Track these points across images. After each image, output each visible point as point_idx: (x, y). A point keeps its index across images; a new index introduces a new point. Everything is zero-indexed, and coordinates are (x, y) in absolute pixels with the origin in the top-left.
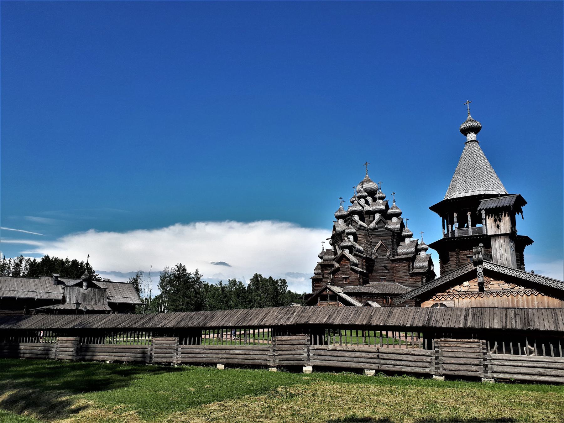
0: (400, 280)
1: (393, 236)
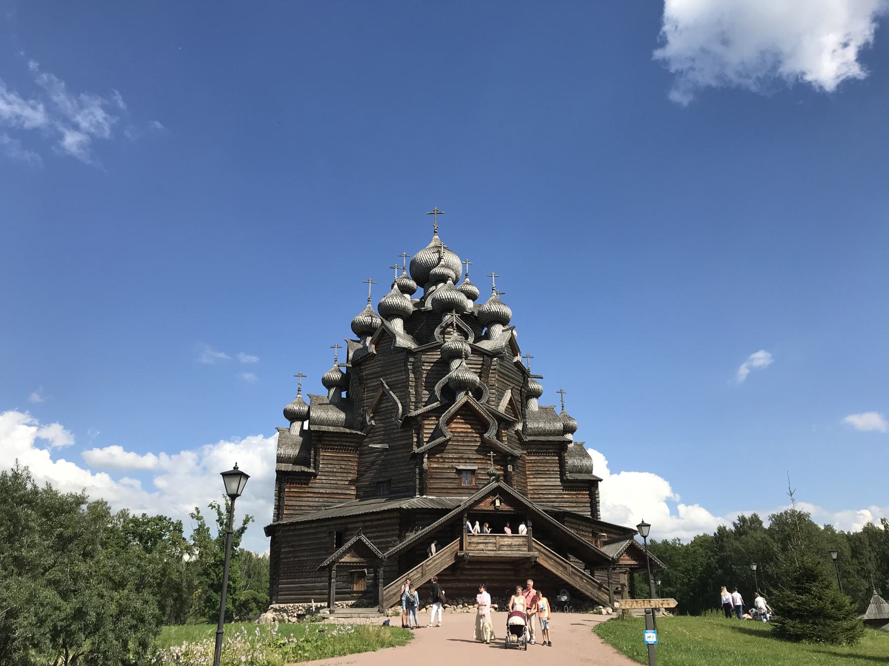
0: (541, 496)
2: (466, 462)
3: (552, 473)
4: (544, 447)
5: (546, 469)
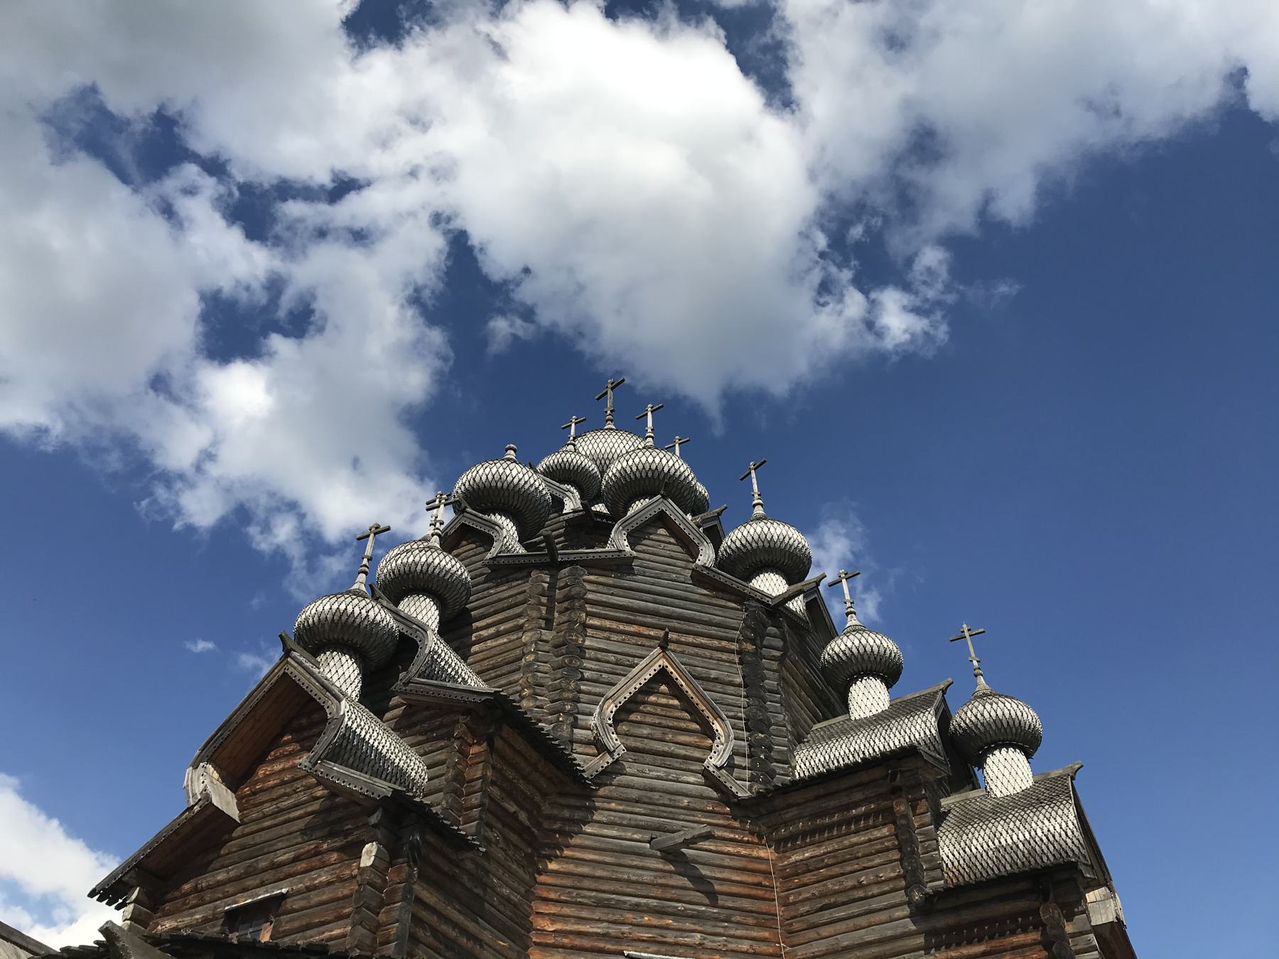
1: (755, 631)
3: (875, 890)
4: (833, 803)
5: (850, 883)
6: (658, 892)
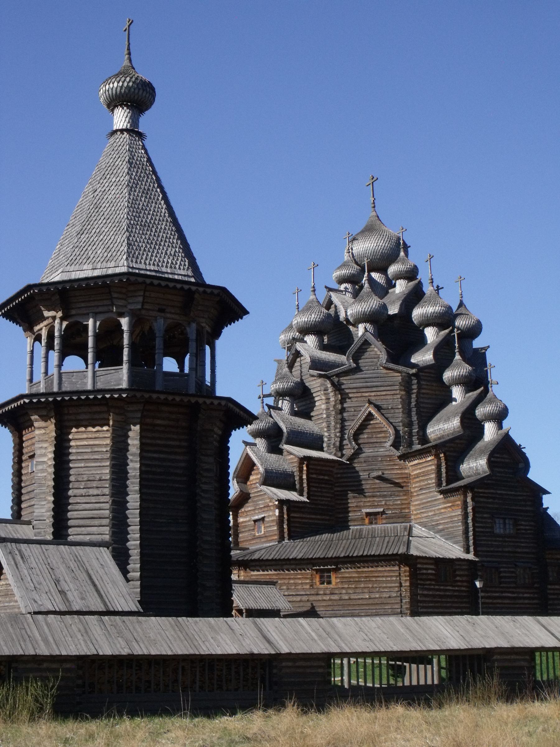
2: (259, 512)
6: (372, 490)
